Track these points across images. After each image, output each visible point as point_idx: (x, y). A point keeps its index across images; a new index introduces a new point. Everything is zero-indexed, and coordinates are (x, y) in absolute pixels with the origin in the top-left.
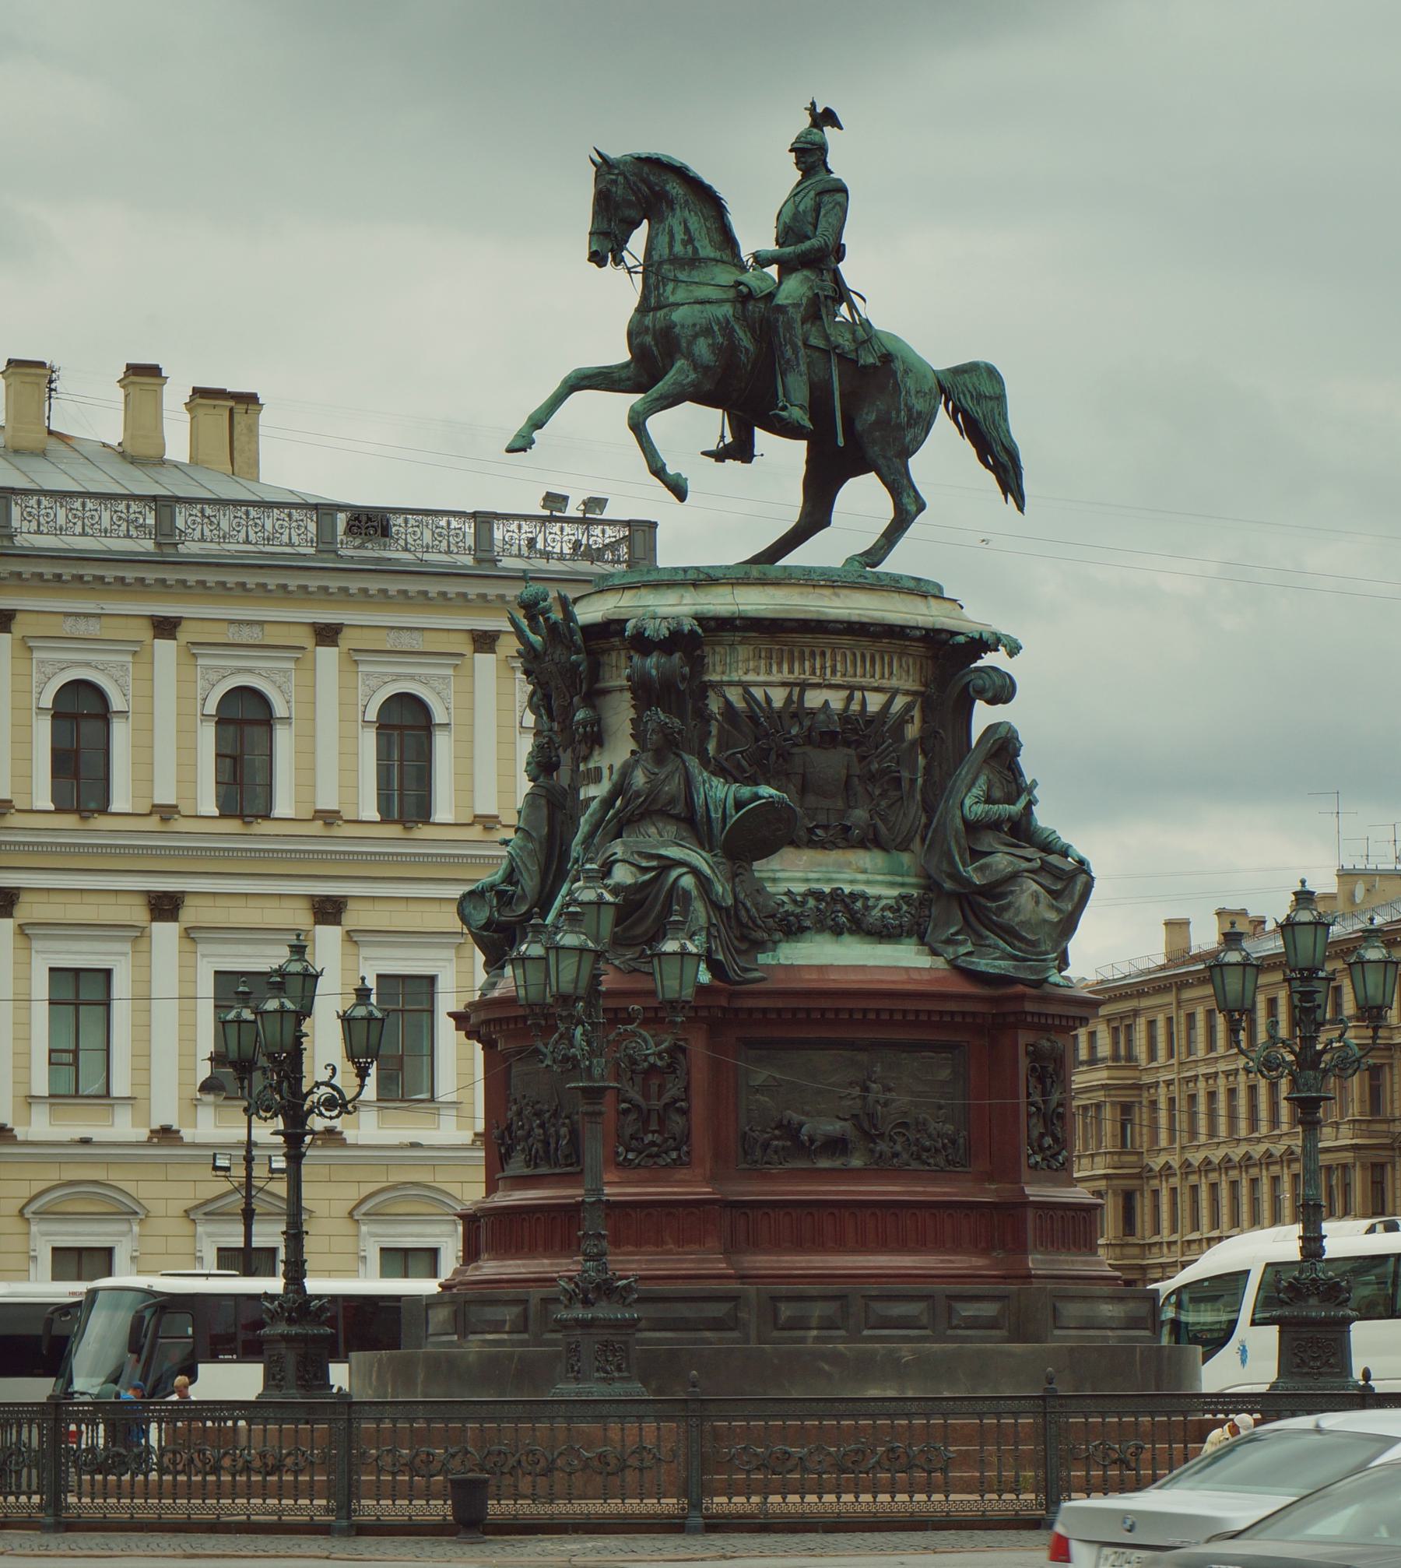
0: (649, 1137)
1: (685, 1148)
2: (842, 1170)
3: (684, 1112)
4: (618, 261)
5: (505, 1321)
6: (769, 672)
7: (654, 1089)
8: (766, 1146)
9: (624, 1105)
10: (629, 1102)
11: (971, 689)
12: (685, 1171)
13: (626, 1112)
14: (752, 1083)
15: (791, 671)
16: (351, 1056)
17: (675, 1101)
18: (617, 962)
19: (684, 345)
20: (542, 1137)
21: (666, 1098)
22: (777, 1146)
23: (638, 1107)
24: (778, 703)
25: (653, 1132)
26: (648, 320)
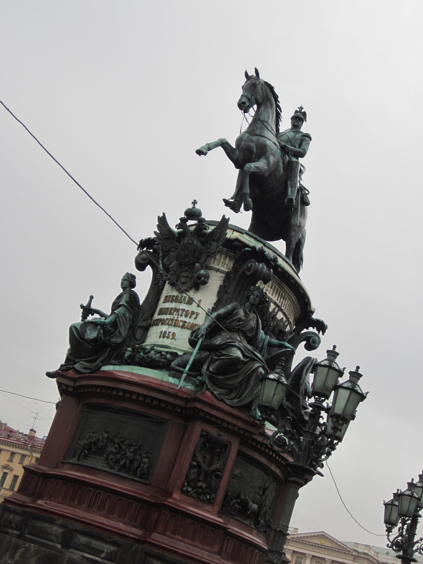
0: (200, 484)
1: (213, 495)
2: (248, 526)
3: (219, 477)
4: (246, 111)
5: (103, 552)
6: (272, 295)
7: (207, 460)
8: (233, 505)
9: (195, 463)
10: (197, 462)
11: (311, 340)
12: (210, 507)
13: (194, 466)
14: (234, 473)
15: (277, 300)
17: (217, 470)
18: (215, 393)
19: (267, 154)
20: (131, 458)
21: (213, 467)
22: (237, 507)
24: (271, 310)
25: (203, 482)
26: (255, 138)
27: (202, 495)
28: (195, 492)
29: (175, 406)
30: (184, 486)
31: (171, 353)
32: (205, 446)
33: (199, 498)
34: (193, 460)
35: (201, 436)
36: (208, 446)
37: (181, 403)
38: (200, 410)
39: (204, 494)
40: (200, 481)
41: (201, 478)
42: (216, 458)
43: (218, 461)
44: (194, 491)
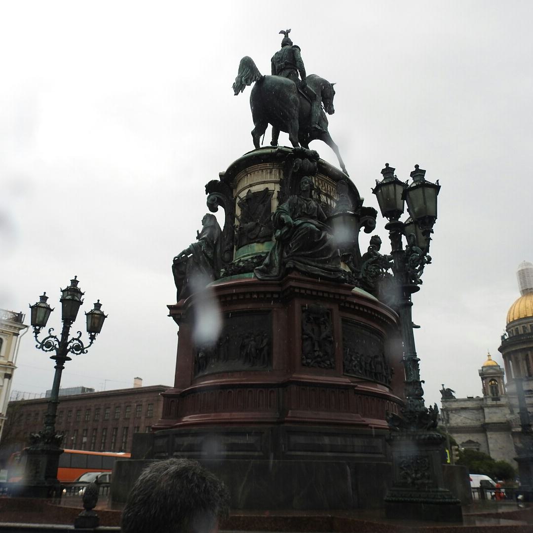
0: (317, 354)
3: (331, 342)
9: (305, 336)
10: (307, 335)
11: (368, 222)
13: (306, 339)
16: (89, 331)
21: (324, 335)
23: (311, 338)
27: (322, 363)
28: (315, 362)
29: (272, 293)
30: (302, 359)
31: (256, 257)
32: (309, 319)
33: (319, 366)
34: (303, 334)
35: (303, 311)
36: (312, 318)
37: (278, 289)
38: (295, 287)
39: (323, 362)
40: (316, 351)
41: (317, 348)
42: (323, 327)
43: (325, 328)
44: (314, 361)
